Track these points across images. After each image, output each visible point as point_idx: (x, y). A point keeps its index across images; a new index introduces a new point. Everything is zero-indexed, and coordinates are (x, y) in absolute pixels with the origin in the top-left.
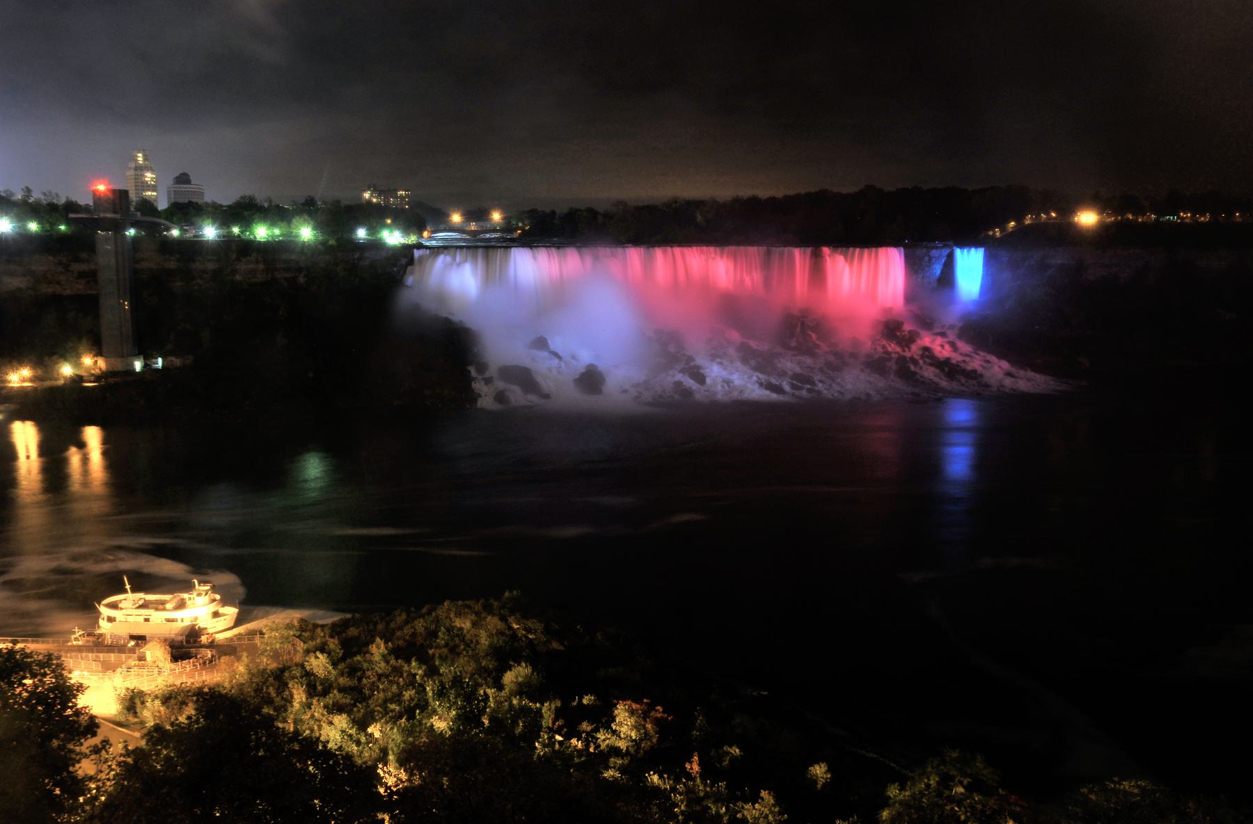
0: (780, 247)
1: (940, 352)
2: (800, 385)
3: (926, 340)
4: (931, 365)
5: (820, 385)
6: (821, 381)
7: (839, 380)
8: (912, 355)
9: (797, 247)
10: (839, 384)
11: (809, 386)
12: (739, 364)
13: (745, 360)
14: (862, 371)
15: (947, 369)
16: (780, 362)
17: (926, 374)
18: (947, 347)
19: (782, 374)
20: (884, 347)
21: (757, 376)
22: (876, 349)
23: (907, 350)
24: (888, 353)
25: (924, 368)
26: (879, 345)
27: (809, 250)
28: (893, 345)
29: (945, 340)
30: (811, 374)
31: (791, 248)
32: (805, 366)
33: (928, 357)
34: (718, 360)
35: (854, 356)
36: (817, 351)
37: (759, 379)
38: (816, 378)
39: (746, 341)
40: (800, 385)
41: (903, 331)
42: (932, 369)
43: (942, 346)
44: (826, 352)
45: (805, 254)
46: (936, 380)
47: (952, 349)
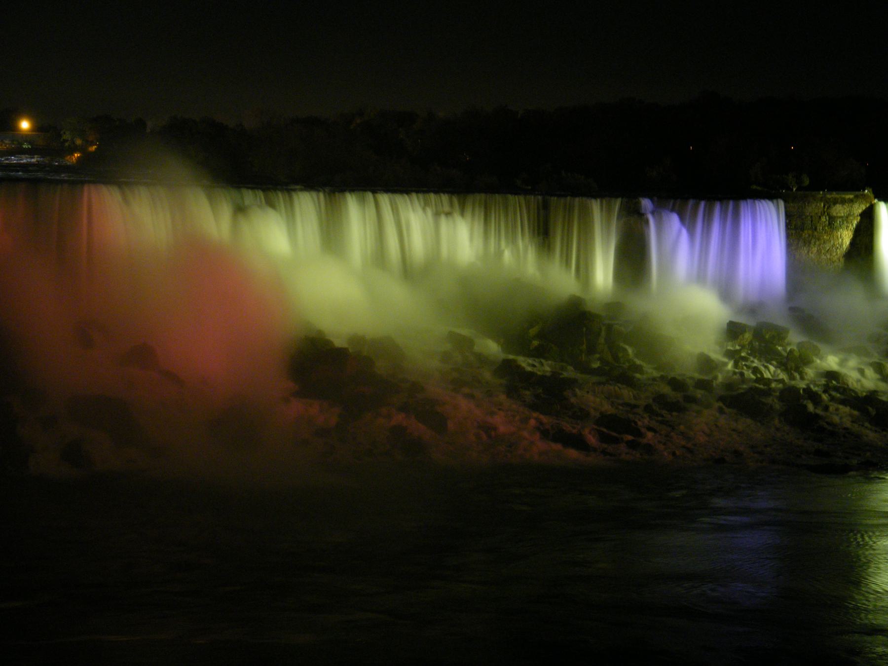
0: (565, 196)
1: (858, 381)
2: (614, 434)
3: (832, 362)
4: (843, 402)
5: (650, 435)
6: (650, 429)
7: (682, 427)
8: (808, 385)
9: (595, 197)
10: (682, 433)
11: (630, 438)
12: (502, 397)
13: (512, 391)
14: (721, 411)
15: (872, 411)
16: (575, 395)
17: (836, 419)
18: (870, 372)
19: (581, 415)
20: (755, 370)
21: (536, 419)
22: (742, 374)
23: (797, 375)
24: (767, 382)
25: (831, 409)
26: (748, 367)
27: (617, 204)
28: (772, 368)
29: (866, 360)
30: (631, 416)
31: (584, 199)
32: (620, 401)
33: (836, 389)
34: (466, 390)
35: (703, 385)
36: (638, 376)
37: (541, 423)
38: (644, 421)
39: (511, 357)
40: (614, 434)
41: (789, 344)
42: (845, 410)
43: (861, 372)
44: (654, 379)
45: (609, 211)
46: (856, 428)
47: (878, 376)
